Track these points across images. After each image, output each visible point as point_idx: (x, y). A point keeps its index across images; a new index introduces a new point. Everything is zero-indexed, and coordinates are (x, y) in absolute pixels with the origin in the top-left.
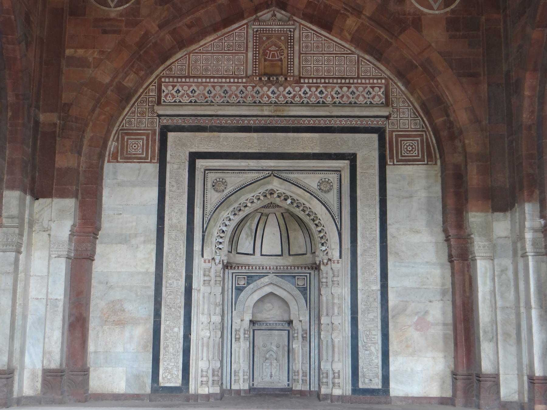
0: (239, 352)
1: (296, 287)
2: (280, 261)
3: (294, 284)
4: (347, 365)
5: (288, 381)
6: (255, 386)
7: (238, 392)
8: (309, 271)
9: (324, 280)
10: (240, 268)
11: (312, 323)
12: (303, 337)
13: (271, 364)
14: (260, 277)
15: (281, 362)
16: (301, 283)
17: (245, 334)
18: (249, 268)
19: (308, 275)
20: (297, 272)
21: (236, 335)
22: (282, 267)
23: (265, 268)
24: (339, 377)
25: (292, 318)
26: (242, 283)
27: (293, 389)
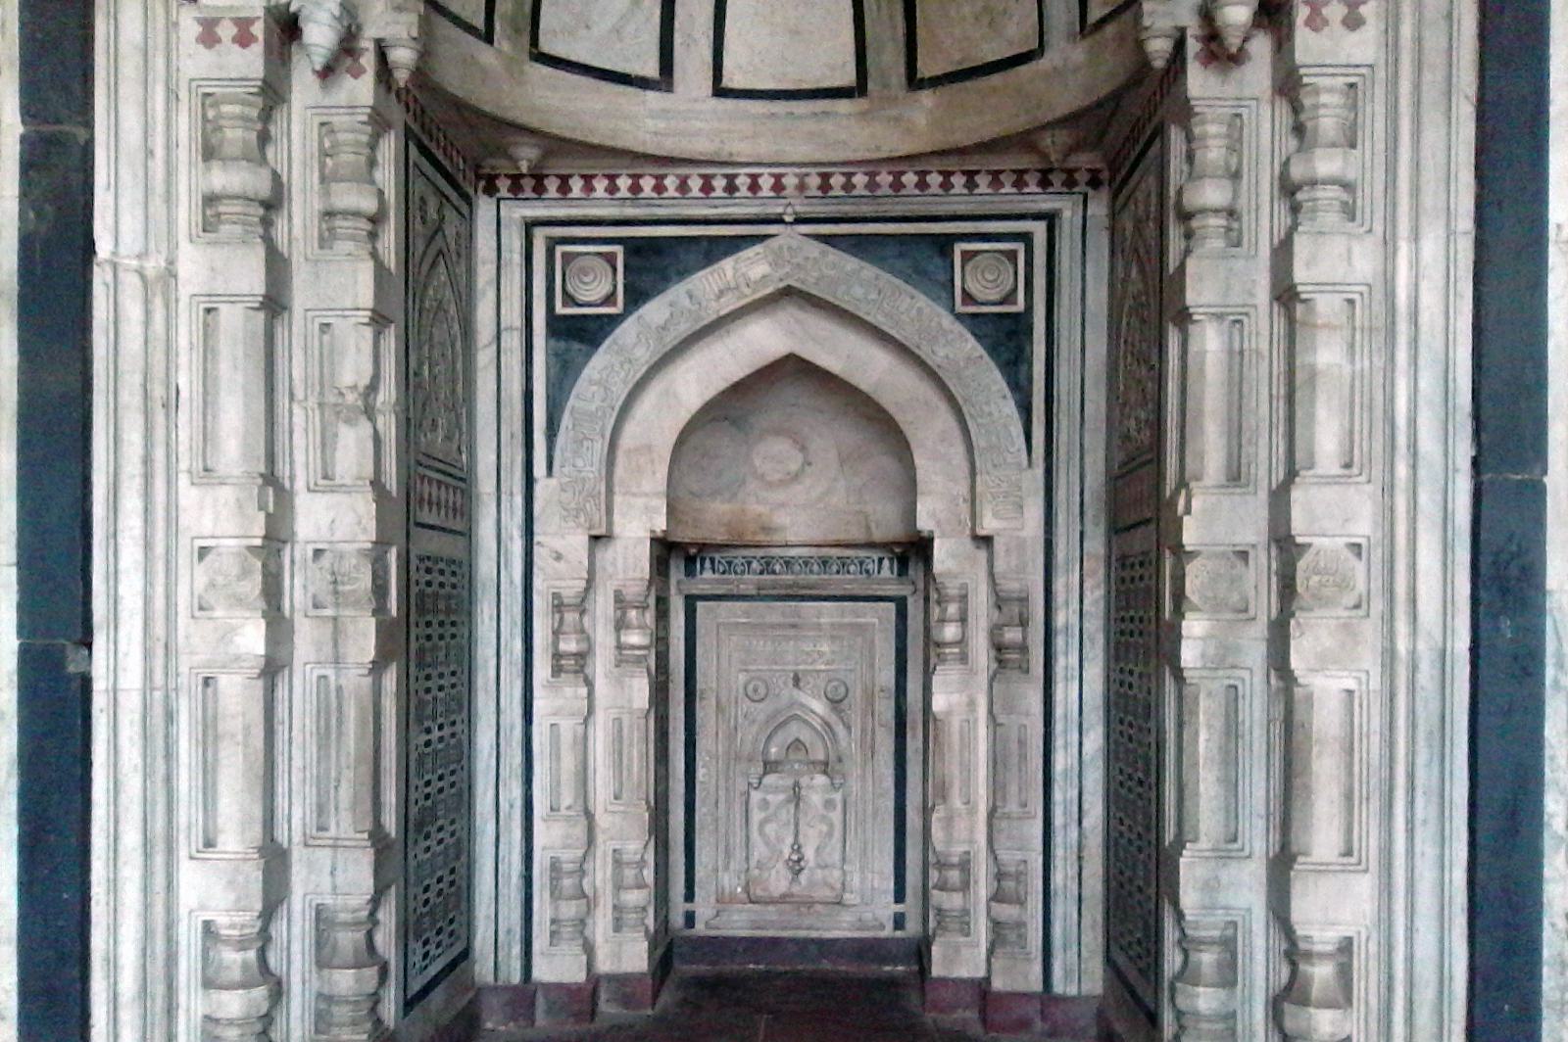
0: (583, 743)
1: (959, 317)
4: (1426, 902)
5: (900, 896)
6: (700, 928)
10: (576, 185)
12: (999, 648)
13: (796, 796)
14: (715, 250)
15: (854, 785)
16: (985, 281)
17: (620, 625)
18: (636, 189)
20: (962, 209)
21: (557, 633)
22: (860, 179)
23: (742, 182)
24: (1343, 995)
25: (924, 523)
26: (595, 286)
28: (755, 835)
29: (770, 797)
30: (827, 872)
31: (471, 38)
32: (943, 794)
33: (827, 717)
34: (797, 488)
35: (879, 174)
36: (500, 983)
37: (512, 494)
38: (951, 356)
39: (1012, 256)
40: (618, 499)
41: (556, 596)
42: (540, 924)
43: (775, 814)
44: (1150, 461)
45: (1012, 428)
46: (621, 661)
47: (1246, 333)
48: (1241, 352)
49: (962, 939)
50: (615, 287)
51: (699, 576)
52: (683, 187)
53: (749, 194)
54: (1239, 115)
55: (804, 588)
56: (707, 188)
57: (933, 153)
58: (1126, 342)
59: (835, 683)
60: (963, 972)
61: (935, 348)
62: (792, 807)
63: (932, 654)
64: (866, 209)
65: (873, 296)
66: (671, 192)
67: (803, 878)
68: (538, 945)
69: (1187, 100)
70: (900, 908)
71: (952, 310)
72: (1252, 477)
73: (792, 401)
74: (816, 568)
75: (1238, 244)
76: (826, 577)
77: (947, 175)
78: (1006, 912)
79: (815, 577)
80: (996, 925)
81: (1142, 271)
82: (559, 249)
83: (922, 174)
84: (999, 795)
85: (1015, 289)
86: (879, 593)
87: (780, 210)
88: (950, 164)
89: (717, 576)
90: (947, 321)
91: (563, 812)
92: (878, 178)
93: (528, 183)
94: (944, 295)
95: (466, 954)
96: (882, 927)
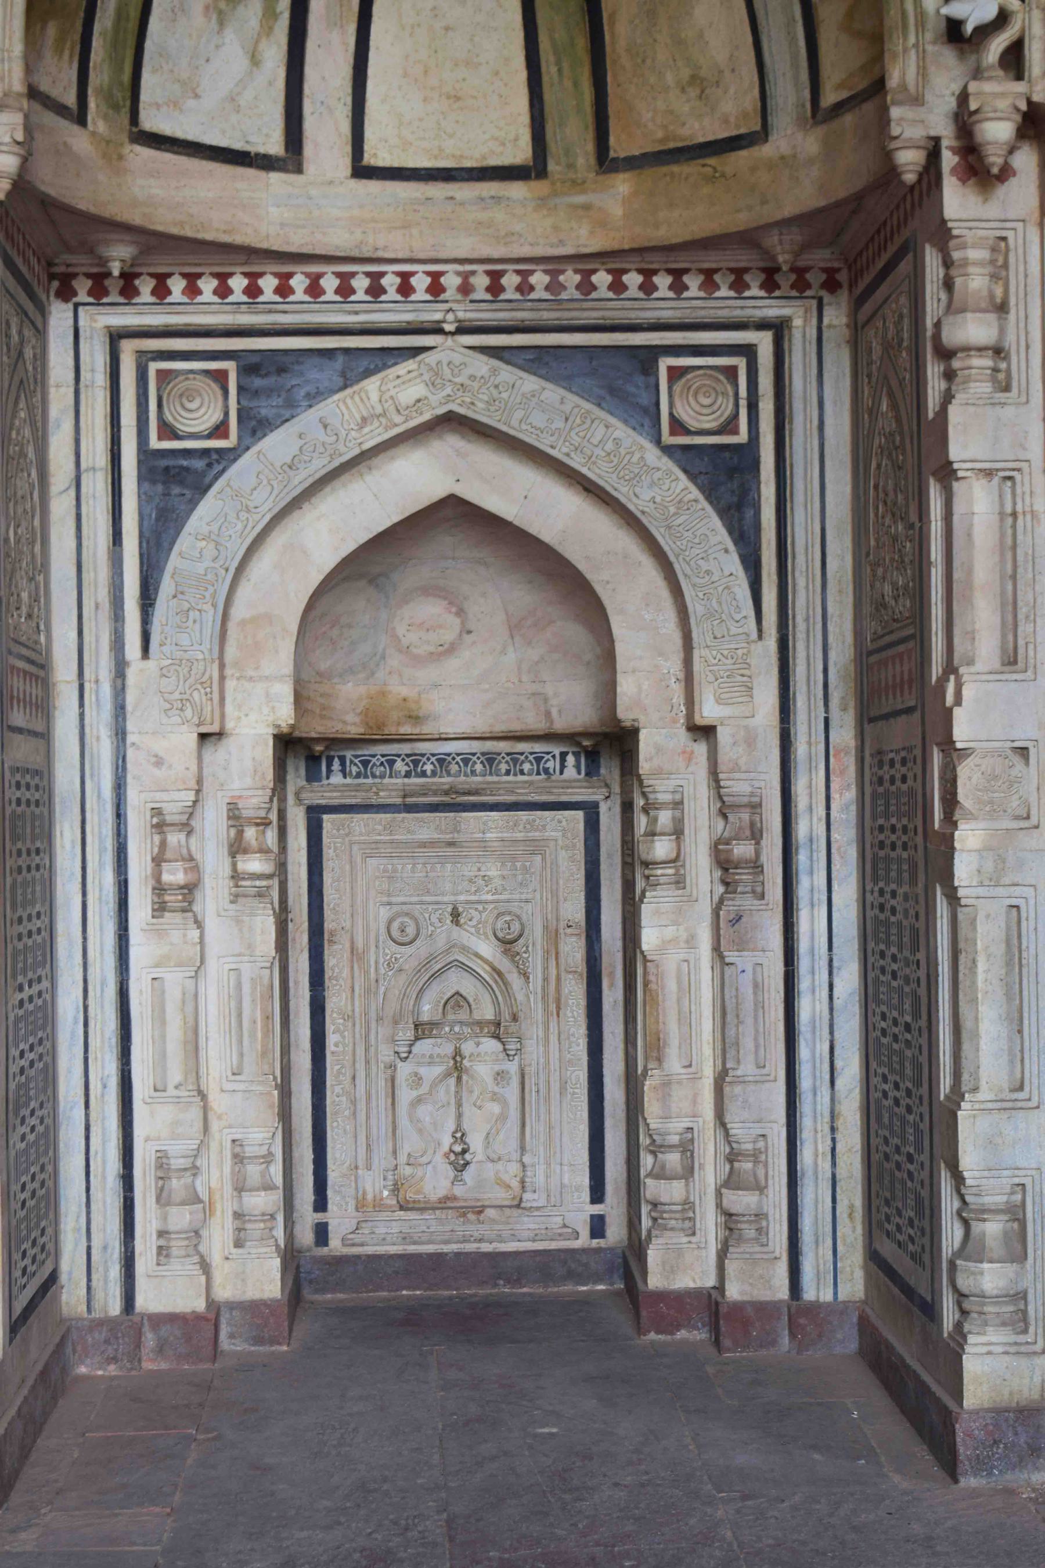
0: (193, 1000)
1: (668, 450)
2: (522, 223)
3: (646, 417)
5: (597, 1194)
7: (198, 1330)
8: (773, 310)
9: (973, 330)
10: (177, 286)
11: (800, 749)
12: (724, 864)
13: (458, 1067)
15: (533, 1050)
17: (237, 848)
18: (253, 291)
19: (763, 341)
21: (158, 860)
22: (539, 279)
23: (390, 282)
25: (625, 713)
26: (199, 414)
27: (655, 1281)
28: (403, 1121)
29: (423, 1071)
30: (500, 1166)
31: (63, 124)
32: (657, 1050)
33: (496, 964)
34: (453, 663)
35: (563, 272)
36: (96, 1315)
37: (97, 681)
38: (658, 499)
39: (731, 373)
40: (230, 684)
41: (157, 812)
42: (144, 1236)
43: (430, 1093)
44: (912, 637)
45: (736, 590)
46: (237, 896)
47: (1019, 491)
48: (1014, 515)
49: (685, 1239)
50: (226, 414)
51: (325, 782)
52: (314, 289)
53: (399, 298)
54: (1004, 239)
55: (464, 794)
56: (345, 290)
57: (633, 250)
58: (876, 487)
59: (508, 918)
60: (684, 1282)
61: (637, 490)
62: (452, 1081)
63: (638, 877)
64: (548, 316)
65: (559, 424)
66: (299, 295)
67: (468, 1175)
68: (143, 1265)
69: (944, 222)
70: (597, 1209)
71: (658, 442)
72: (1031, 661)
73: (452, 556)
74: (479, 767)
75: (1007, 389)
76: (495, 778)
77: (648, 274)
78: (741, 1201)
79: (479, 779)
80: (729, 1219)
81: (894, 406)
82: (153, 367)
83: (618, 274)
84: (731, 1054)
85: (735, 416)
86: (564, 798)
87: (438, 316)
88: (654, 261)
89: (348, 781)
90: (652, 455)
91: (171, 1091)
92: (561, 278)
93: (114, 286)
94: (647, 422)
95: (53, 1278)
96: (576, 1235)
